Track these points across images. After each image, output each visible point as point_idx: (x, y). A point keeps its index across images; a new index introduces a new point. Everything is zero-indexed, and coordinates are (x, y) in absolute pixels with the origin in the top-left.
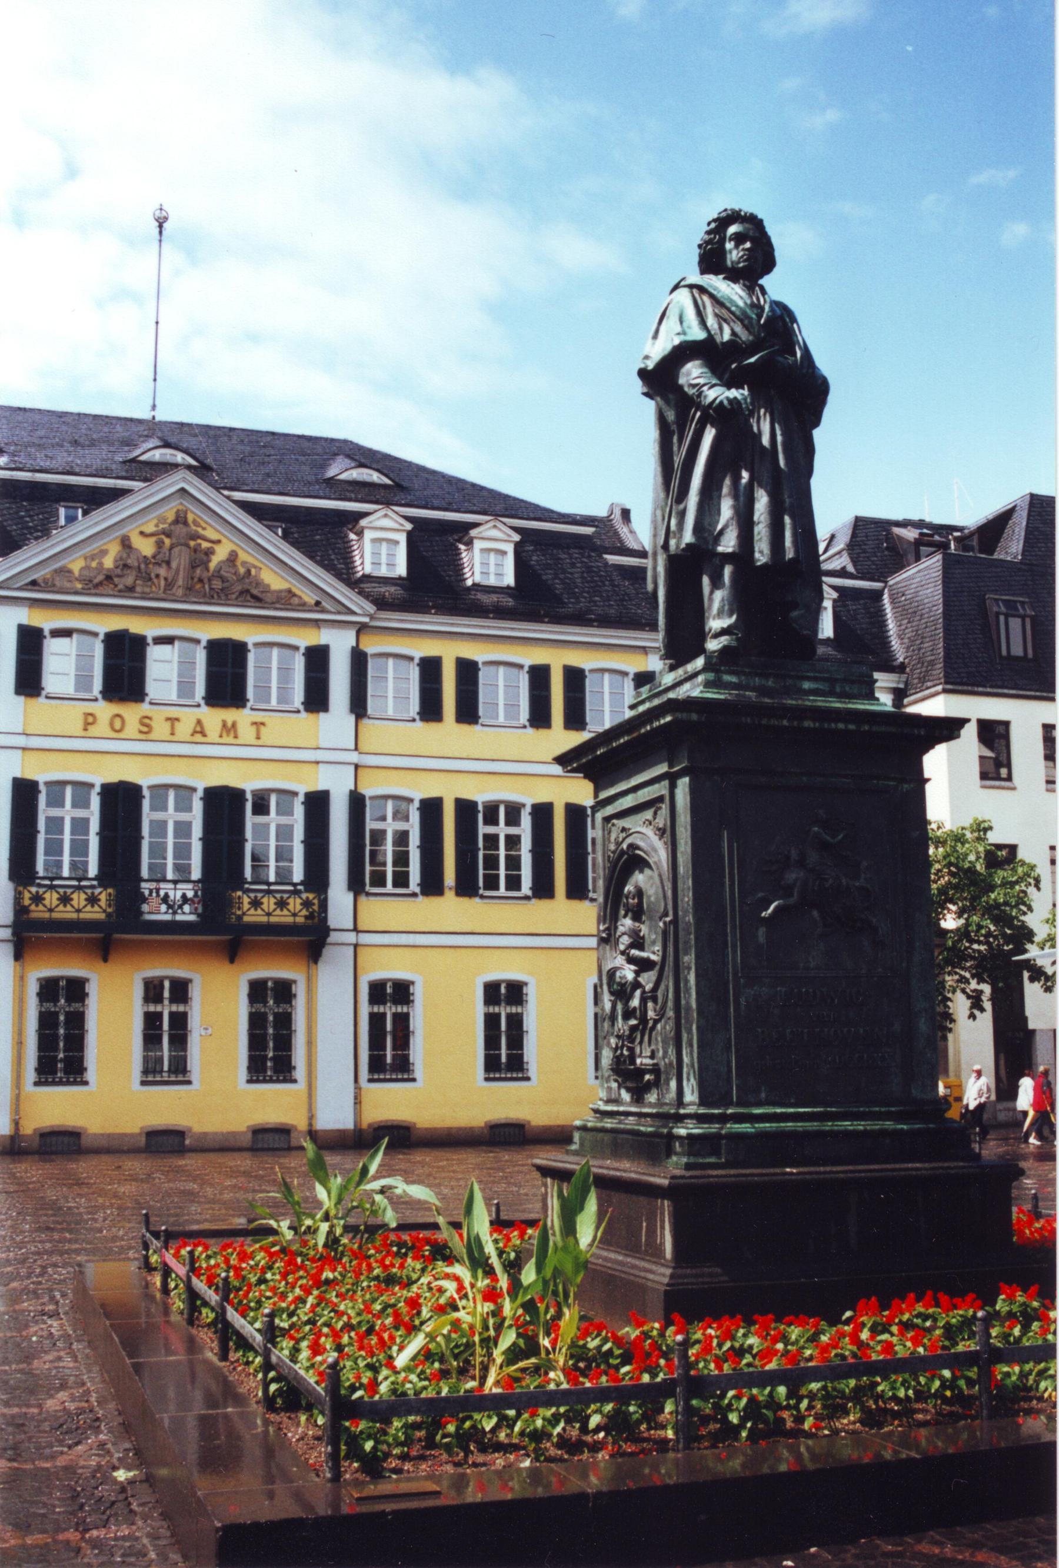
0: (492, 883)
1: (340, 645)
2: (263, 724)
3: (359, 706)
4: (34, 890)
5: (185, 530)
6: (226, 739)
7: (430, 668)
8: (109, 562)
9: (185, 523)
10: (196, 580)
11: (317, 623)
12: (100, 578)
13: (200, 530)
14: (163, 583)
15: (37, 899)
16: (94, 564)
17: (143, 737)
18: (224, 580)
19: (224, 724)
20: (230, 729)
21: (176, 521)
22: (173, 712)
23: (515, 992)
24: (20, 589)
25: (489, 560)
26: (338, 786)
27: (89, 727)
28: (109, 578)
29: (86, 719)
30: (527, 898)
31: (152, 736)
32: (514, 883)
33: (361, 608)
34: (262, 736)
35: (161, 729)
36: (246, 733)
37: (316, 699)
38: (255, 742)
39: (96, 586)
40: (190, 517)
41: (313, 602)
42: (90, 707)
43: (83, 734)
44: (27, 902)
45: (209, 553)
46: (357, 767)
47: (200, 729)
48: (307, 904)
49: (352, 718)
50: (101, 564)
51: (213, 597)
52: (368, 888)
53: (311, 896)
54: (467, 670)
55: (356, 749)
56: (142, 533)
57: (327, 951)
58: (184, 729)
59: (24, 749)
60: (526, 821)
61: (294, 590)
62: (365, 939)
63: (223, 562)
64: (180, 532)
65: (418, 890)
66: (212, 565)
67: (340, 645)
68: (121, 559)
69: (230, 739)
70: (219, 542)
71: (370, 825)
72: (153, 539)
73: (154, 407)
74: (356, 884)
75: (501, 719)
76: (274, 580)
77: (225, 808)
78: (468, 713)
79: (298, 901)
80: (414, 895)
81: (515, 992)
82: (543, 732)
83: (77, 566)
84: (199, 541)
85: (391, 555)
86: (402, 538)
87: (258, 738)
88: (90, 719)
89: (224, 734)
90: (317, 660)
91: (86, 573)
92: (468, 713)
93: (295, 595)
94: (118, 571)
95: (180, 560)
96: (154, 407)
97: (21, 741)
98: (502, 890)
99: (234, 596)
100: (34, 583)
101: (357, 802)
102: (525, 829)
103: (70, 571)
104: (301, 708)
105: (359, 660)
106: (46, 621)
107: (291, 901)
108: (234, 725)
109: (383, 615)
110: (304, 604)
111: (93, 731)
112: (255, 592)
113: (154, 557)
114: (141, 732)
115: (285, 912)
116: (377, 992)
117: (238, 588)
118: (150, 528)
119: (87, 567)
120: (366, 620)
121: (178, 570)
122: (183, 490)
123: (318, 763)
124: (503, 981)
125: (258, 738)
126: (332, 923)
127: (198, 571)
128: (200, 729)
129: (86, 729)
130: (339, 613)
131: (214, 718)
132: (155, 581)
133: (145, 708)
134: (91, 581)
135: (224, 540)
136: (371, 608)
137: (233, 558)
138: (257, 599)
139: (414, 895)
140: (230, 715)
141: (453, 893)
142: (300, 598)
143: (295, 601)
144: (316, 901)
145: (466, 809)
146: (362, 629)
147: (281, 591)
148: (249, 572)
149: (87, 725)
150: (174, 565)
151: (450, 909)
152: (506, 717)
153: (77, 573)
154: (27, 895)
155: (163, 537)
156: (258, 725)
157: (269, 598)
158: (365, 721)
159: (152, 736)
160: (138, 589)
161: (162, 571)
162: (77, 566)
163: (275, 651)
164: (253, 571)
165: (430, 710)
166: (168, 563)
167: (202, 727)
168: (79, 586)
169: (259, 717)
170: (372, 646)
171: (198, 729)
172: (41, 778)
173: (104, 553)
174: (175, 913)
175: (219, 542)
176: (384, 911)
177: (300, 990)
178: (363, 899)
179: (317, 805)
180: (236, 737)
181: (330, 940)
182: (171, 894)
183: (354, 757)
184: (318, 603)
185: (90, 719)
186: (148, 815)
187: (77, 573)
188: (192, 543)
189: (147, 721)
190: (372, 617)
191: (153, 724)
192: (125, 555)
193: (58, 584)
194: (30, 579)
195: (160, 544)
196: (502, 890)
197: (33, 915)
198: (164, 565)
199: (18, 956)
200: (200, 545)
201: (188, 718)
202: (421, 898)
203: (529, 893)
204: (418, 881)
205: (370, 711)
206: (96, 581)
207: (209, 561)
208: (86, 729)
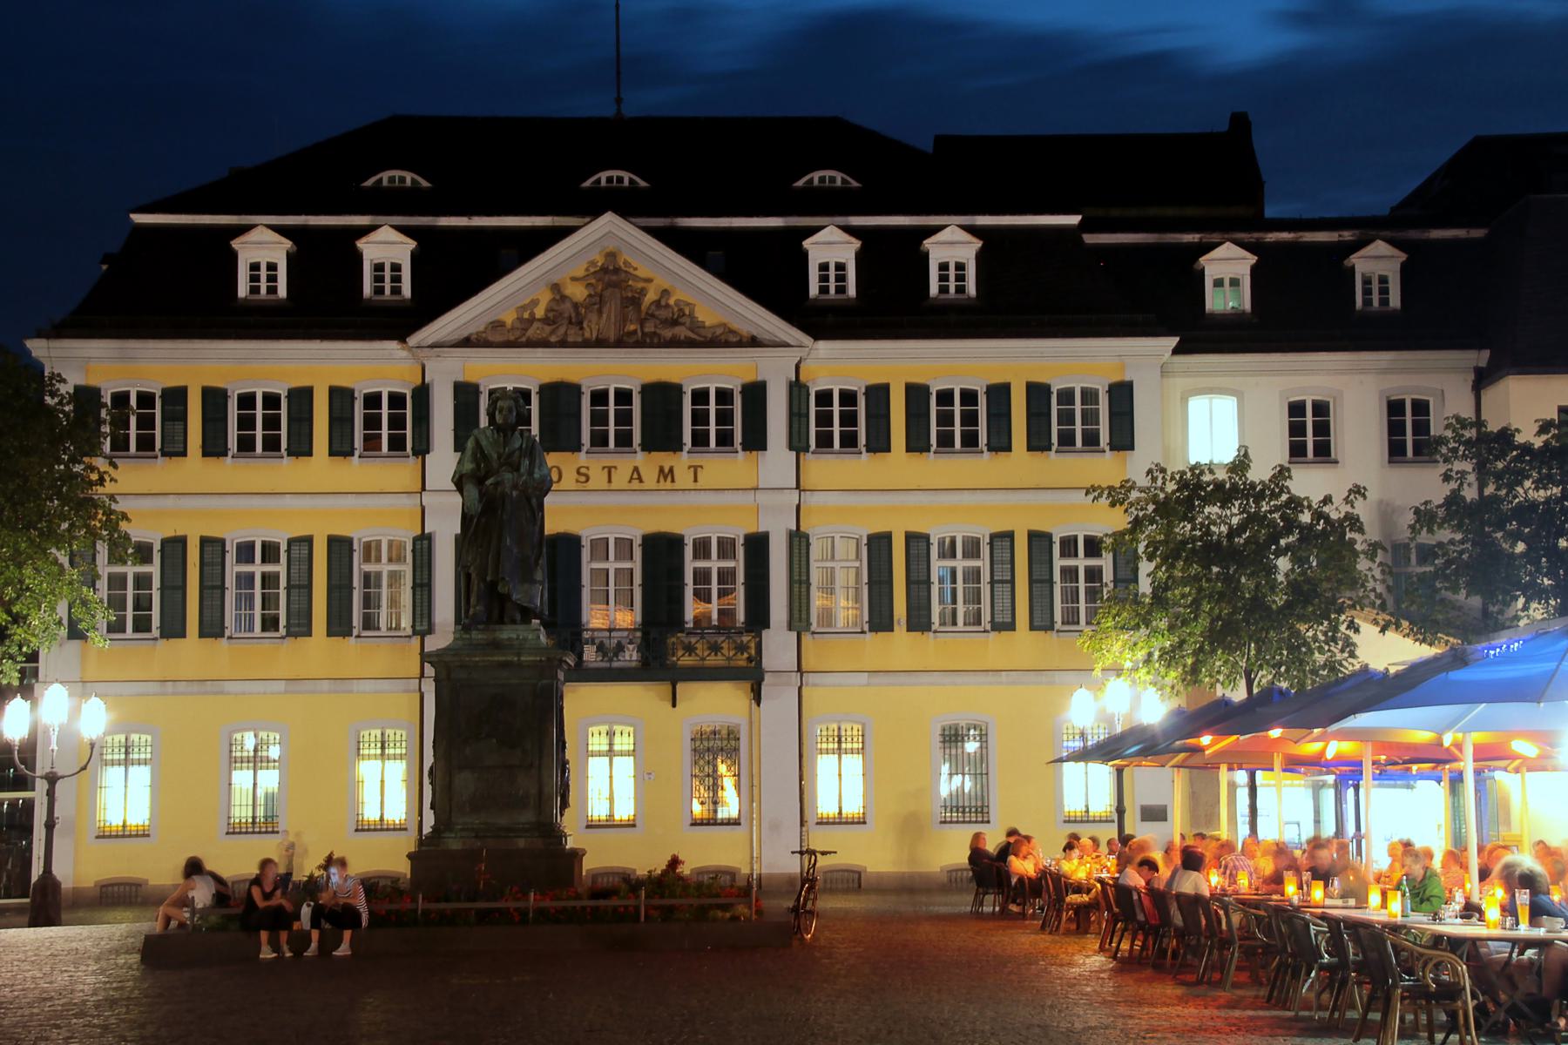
6: (662, 485)
8: (540, 312)
17: (580, 486)
19: (661, 470)
20: (667, 474)
22: (608, 460)
31: (590, 485)
35: (598, 479)
36: (683, 478)
37: (756, 440)
38: (691, 485)
45: (643, 292)
47: (636, 474)
50: (532, 314)
52: (814, 627)
55: (798, 487)
58: (621, 478)
64: (610, 275)
69: (668, 485)
74: (799, 620)
76: (707, 316)
77: (662, 553)
80: (863, 632)
83: (509, 318)
87: (696, 480)
90: (755, 394)
108: (671, 470)
115: (719, 657)
118: (581, 273)
125: (696, 480)
128: (636, 474)
131: (648, 463)
133: (582, 458)
136: (807, 340)
140: (665, 459)
144: (753, 645)
156: (696, 469)
159: (590, 485)
169: (698, 459)
173: (535, 303)
174: (611, 660)
179: (757, 545)
182: (606, 642)
186: (588, 566)
191: (590, 473)
201: (624, 464)
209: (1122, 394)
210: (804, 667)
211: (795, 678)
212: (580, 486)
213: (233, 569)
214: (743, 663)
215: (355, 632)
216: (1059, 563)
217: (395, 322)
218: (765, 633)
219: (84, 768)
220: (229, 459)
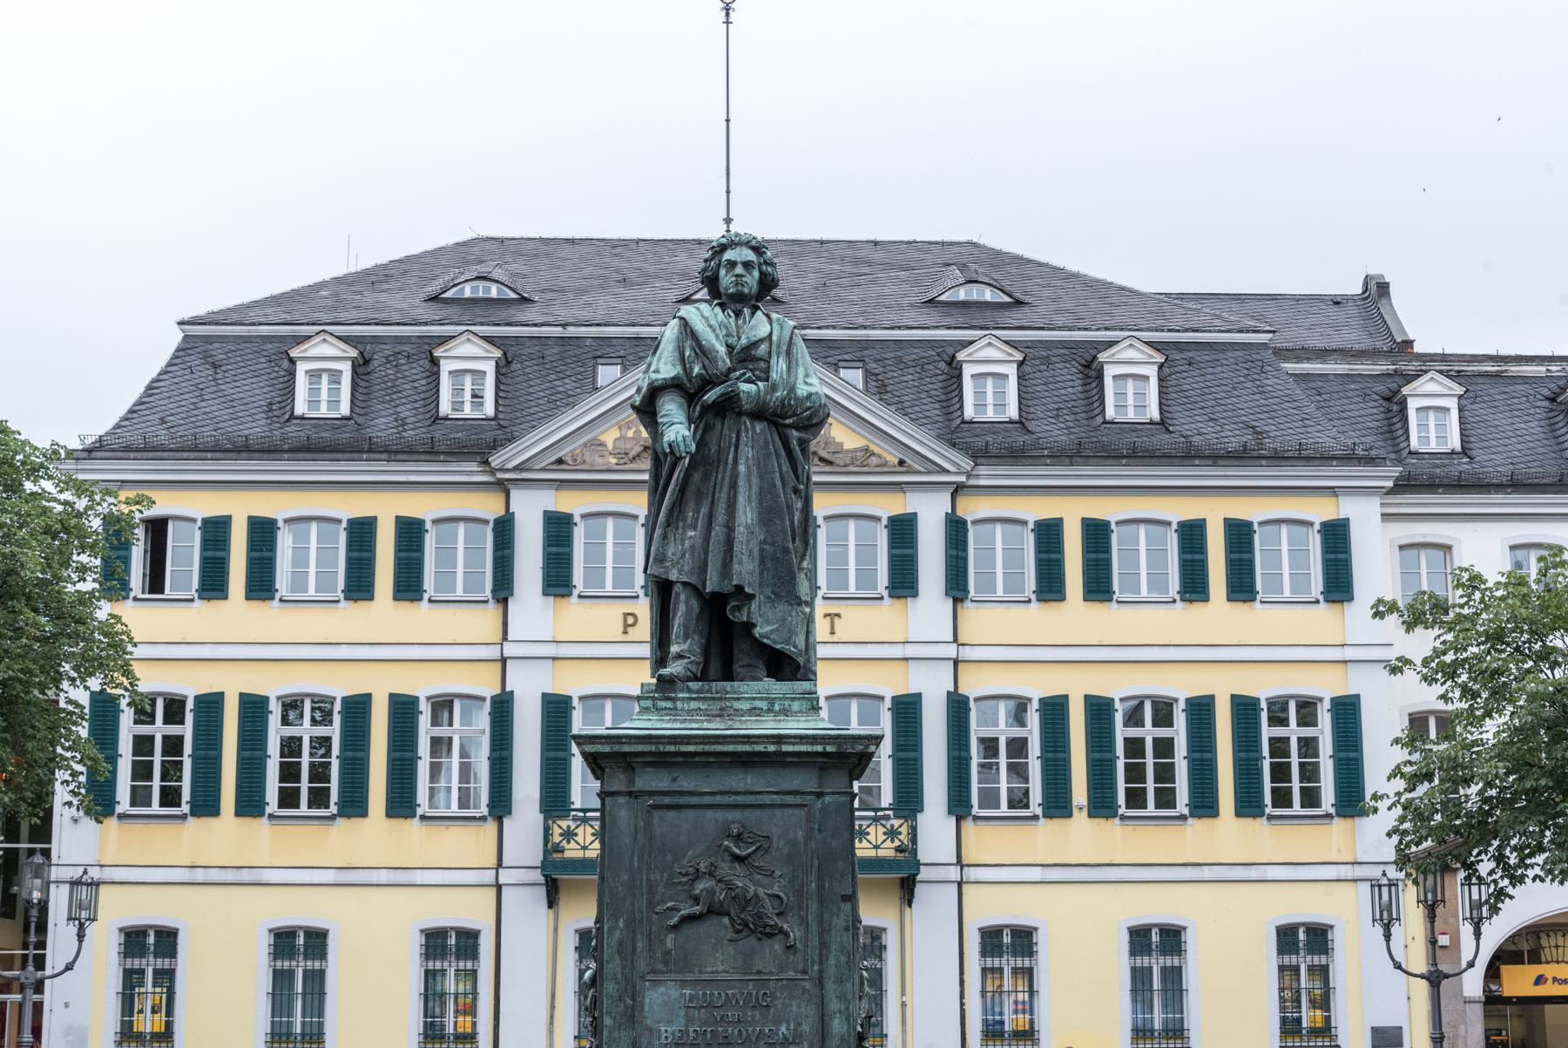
0: (1136, 798)
1: (931, 513)
2: (838, 615)
3: (957, 586)
4: (564, 824)
7: (1049, 534)
11: (899, 487)
12: (638, 449)
15: (569, 835)
16: (630, 434)
23: (1172, 938)
24: (543, 470)
25: (1132, 391)
26: (933, 689)
30: (1183, 818)
32: (1166, 799)
33: (954, 463)
34: (837, 629)
37: (903, 582)
41: (896, 461)
42: (628, 607)
44: (557, 839)
46: (956, 662)
48: (892, 834)
49: (949, 604)
52: (975, 810)
53: (896, 823)
54: (1097, 533)
55: (955, 640)
57: (919, 889)
59: (554, 659)
60: (1180, 719)
62: (973, 873)
65: (1039, 811)
67: (931, 513)
71: (976, 731)
73: (728, 221)
74: (959, 805)
75: (1144, 593)
78: (1098, 587)
79: (881, 830)
80: (1036, 818)
81: (1172, 938)
82: (1197, 608)
83: (610, 437)
85: (1000, 394)
86: (1011, 371)
87: (832, 633)
88: (630, 620)
90: (903, 531)
91: (621, 444)
93: (873, 454)
96: (728, 221)
97: (550, 650)
98: (1151, 809)
100: (560, 461)
101: (958, 707)
102: (1179, 732)
103: (603, 444)
104: (885, 593)
105: (956, 530)
106: (573, 503)
107: (871, 830)
109: (982, 470)
110: (885, 464)
111: (634, 634)
112: (823, 454)
116: (991, 939)
119: (623, 438)
120: (962, 479)
123: (906, 659)
124: (1155, 925)
125: (832, 633)
126: (923, 856)
129: (625, 632)
130: (929, 473)
136: (967, 464)
138: (830, 463)
139: (1036, 818)
141: (1085, 812)
142: (880, 456)
143: (874, 460)
144: (904, 830)
145: (1099, 710)
146: (958, 490)
147: (855, 450)
149: (626, 627)
151: (1081, 835)
152: (1150, 590)
153: (610, 446)
154: (557, 831)
158: (968, 604)
162: (610, 437)
163: (852, 525)
168: (614, 461)
169: (833, 608)
170: (972, 508)
172: (575, 693)
176: (984, 841)
177: (891, 940)
178: (969, 827)
179: (907, 710)
181: (919, 878)
183: (951, 651)
184: (901, 463)
185: (630, 620)
187: (610, 446)
190: (969, 476)
193: (587, 459)
194: (553, 459)
196: (1151, 809)
197: (568, 854)
199: (551, 903)
202: (1042, 821)
203: (1186, 811)
204: (1040, 801)
205: (972, 593)
208: (625, 632)
209: (1336, 537)
210: (965, 861)
211: (954, 873)
213: (275, 732)
214: (890, 853)
215: (420, 811)
216: (1267, 732)
217: (475, 445)
218: (919, 816)
219: (69, 967)
220: (276, 603)
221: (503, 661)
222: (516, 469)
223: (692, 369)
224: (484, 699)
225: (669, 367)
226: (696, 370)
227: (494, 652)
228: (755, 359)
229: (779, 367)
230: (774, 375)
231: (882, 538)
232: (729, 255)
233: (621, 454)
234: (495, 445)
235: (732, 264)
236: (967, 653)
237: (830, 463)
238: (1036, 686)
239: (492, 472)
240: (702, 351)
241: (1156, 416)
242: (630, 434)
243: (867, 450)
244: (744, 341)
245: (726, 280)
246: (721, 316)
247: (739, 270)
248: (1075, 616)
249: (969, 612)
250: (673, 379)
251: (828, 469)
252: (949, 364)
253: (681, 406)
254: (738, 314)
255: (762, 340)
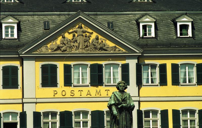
5: (81, 30)
7: (163, 68)
9: (81, 28)
10: (85, 46)
13: (86, 29)
14: (75, 47)
17: (72, 97)
18: (94, 45)
20: (98, 92)
21: (79, 28)
27: (55, 95)
28: (59, 48)
29: (54, 93)
39: (55, 50)
40: (83, 26)
43: (54, 97)
45: (89, 37)
51: (91, 51)
54: (175, 68)
56: (68, 32)
59: (36, 103)
61: (117, 46)
63: (94, 39)
66: (91, 41)
68: (62, 41)
70: (92, 33)
72: (71, 35)
84: (86, 33)
89: (97, 94)
91: (52, 46)
92: (176, 82)
94: (61, 45)
95: (80, 40)
97: (35, 100)
99: (98, 50)
111: (56, 96)
112: (104, 48)
113: (72, 40)
114: (71, 95)
117: (99, 47)
121: (79, 44)
122: (80, 17)
127: (86, 43)
131: (93, 90)
132: (73, 47)
134: (53, 49)
135: (94, 32)
137: (97, 39)
146: (138, 58)
148: (102, 42)
150: (78, 42)
153: (49, 47)
155: (75, 33)
157: (108, 49)
159: (74, 97)
160: (68, 50)
161: (76, 44)
164: (104, 41)
165: (163, 82)
166: (76, 41)
167: (90, 93)
168: (50, 51)
171: (89, 93)
175: (92, 33)
180: (100, 95)
185: (55, 92)
188: (84, 34)
189: (72, 92)
191: (74, 92)
192: (63, 40)
195: (74, 36)
198: (75, 42)
200: (86, 35)
201: (85, 90)
206: (55, 49)
207: (90, 39)
212: (72, 97)
221: (23, 103)
222: (25, 54)
223: (116, 102)
224: (17, 113)
225: (113, 102)
226: (117, 102)
227: (20, 101)
228: (125, 100)
229: (128, 101)
230: (128, 103)
231: (120, 70)
232: (120, 85)
233: (52, 49)
234: (19, 47)
235: (121, 86)
236: (141, 99)
237: (106, 50)
238: (160, 107)
239: (19, 55)
240: (118, 100)
241: (191, 36)
242: (54, 43)
243: (115, 47)
244: (123, 98)
245: (120, 88)
246: (120, 94)
247: (122, 87)
248: (170, 89)
249: (143, 89)
250: (114, 104)
251: (105, 52)
252: (136, 21)
253: (115, 107)
254: (122, 93)
255: (126, 98)
